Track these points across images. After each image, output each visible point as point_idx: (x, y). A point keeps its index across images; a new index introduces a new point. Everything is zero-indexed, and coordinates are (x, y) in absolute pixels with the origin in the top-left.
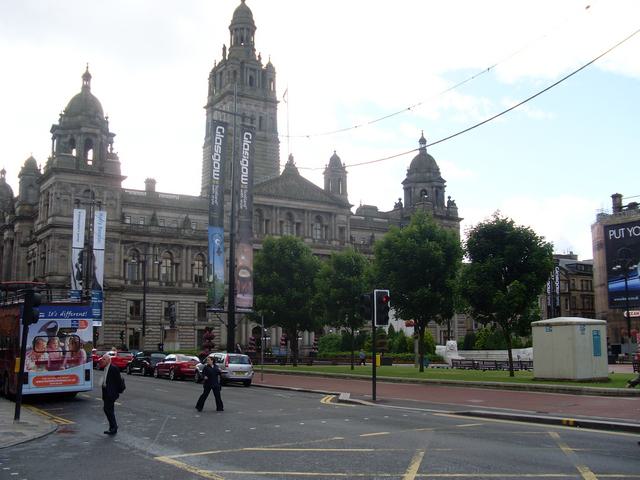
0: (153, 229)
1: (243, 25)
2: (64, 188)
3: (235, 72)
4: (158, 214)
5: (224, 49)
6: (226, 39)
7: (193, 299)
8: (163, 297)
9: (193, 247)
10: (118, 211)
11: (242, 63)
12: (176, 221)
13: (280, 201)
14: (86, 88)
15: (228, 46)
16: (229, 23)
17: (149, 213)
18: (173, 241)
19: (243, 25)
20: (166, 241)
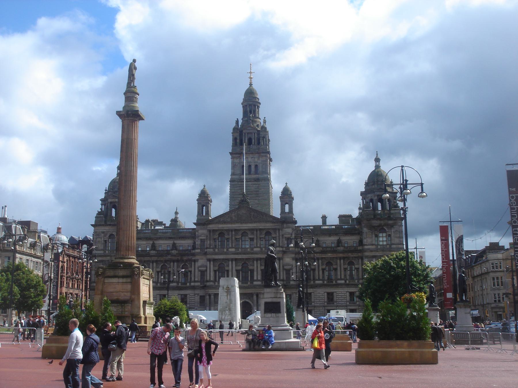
2: (98, 235)
4: (156, 242)
5: (237, 122)
7: (177, 292)
13: (234, 225)
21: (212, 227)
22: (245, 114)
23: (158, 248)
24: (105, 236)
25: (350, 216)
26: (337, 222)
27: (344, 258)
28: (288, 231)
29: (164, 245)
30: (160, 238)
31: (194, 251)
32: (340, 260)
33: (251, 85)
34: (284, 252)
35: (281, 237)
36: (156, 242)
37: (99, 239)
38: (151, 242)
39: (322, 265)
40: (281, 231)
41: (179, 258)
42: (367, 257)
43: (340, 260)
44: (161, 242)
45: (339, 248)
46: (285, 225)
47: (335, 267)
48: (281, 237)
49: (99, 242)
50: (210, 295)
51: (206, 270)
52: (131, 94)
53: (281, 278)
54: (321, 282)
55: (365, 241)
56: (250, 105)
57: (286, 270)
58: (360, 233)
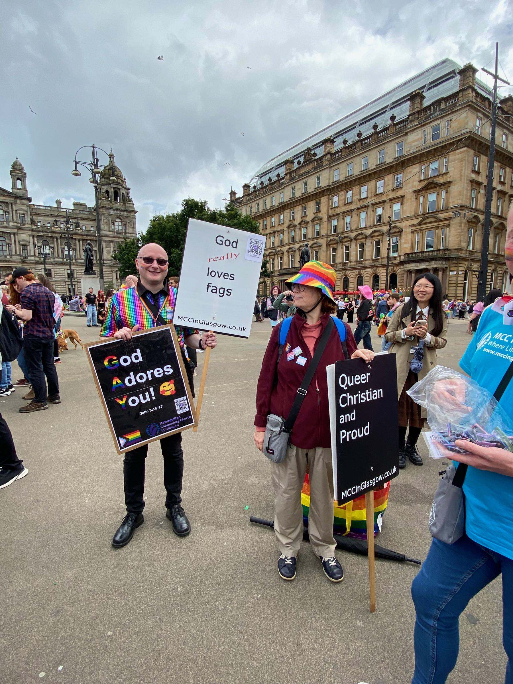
27: (83, 240)
28: (21, 206)
32: (79, 242)
34: (19, 229)
35: (14, 212)
39: (61, 244)
40: (13, 206)
42: (105, 241)
43: (79, 242)
46: (18, 201)
47: (74, 247)
48: (14, 212)
53: (18, 253)
54: (61, 260)
55: (104, 227)
57: (22, 245)
58: (97, 220)
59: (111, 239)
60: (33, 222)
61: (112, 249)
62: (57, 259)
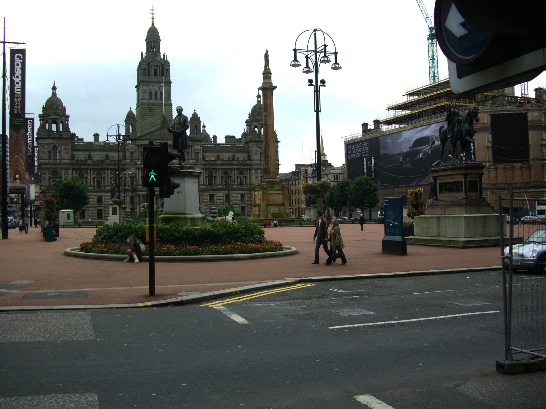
0: (89, 161)
1: (153, 39)
2: (42, 146)
3: (145, 69)
5: (142, 54)
6: (143, 48)
8: (96, 194)
9: (111, 169)
10: (70, 155)
11: (149, 64)
12: (102, 157)
14: (54, 94)
15: (144, 52)
16: (145, 38)
17: (88, 153)
18: (99, 167)
19: (153, 39)
20: (96, 167)
21: (139, 142)
22: (149, 48)
23: (111, 158)
24: (49, 147)
25: (234, 137)
26: (224, 142)
29: (98, 156)
30: (79, 150)
31: (124, 162)
33: (153, 24)
34: (195, 164)
36: (92, 153)
37: (44, 150)
38: (106, 153)
41: (112, 167)
42: (254, 169)
44: (96, 153)
45: (234, 162)
49: (43, 152)
50: (139, 197)
51: (136, 176)
52: (267, 74)
56: (154, 42)
59: (259, 167)
60: (204, 158)
61: (259, 175)
62: (219, 187)
